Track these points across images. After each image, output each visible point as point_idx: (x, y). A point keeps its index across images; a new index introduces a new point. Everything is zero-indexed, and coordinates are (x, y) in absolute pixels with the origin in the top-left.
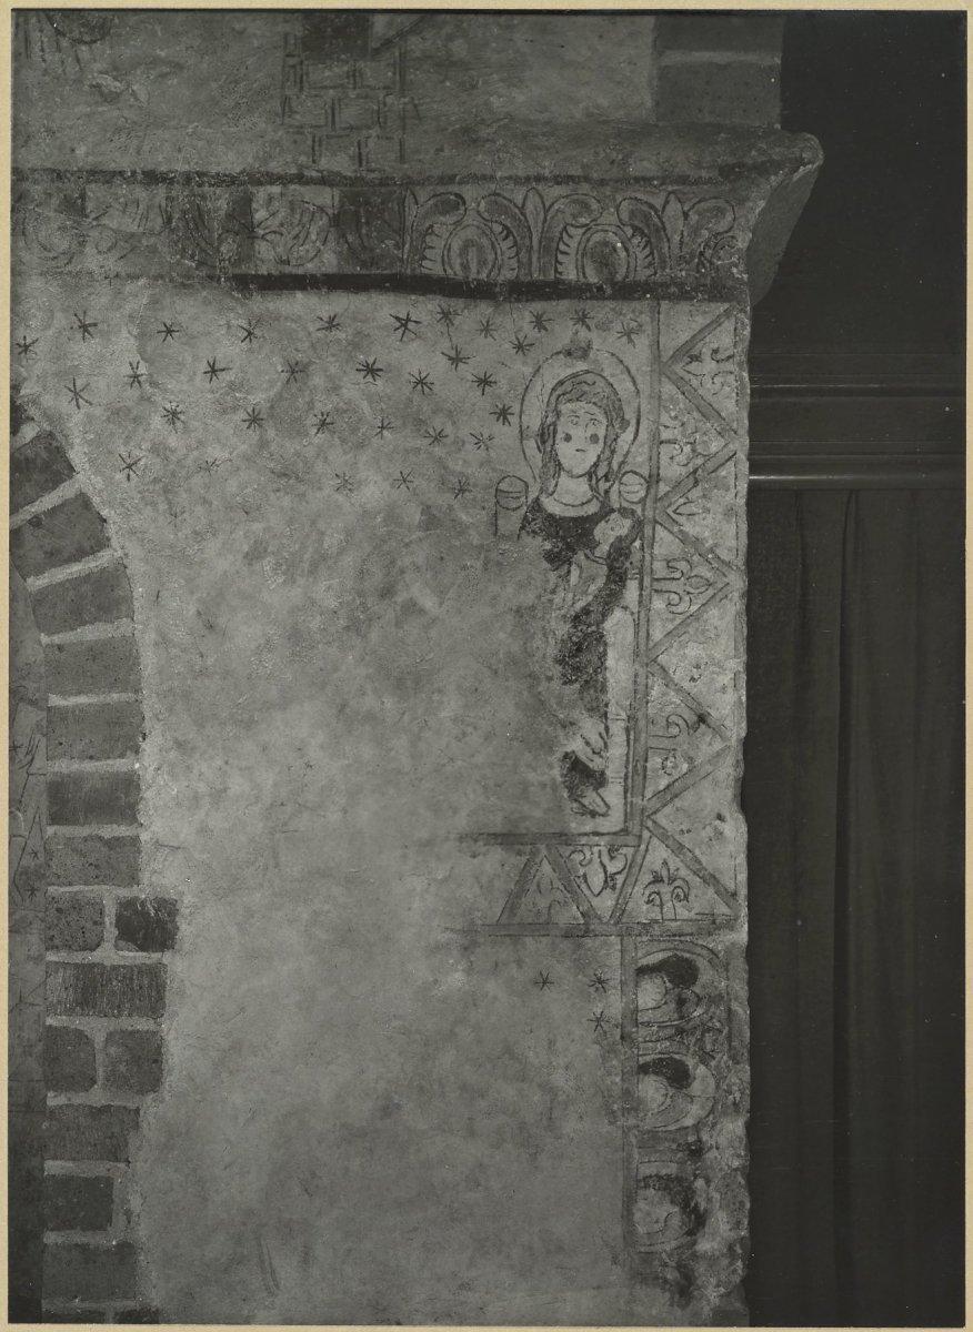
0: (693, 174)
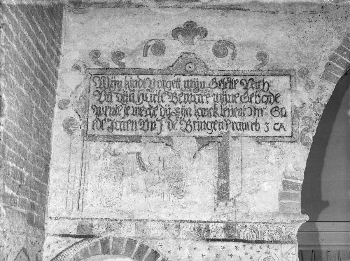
0: (287, 222)
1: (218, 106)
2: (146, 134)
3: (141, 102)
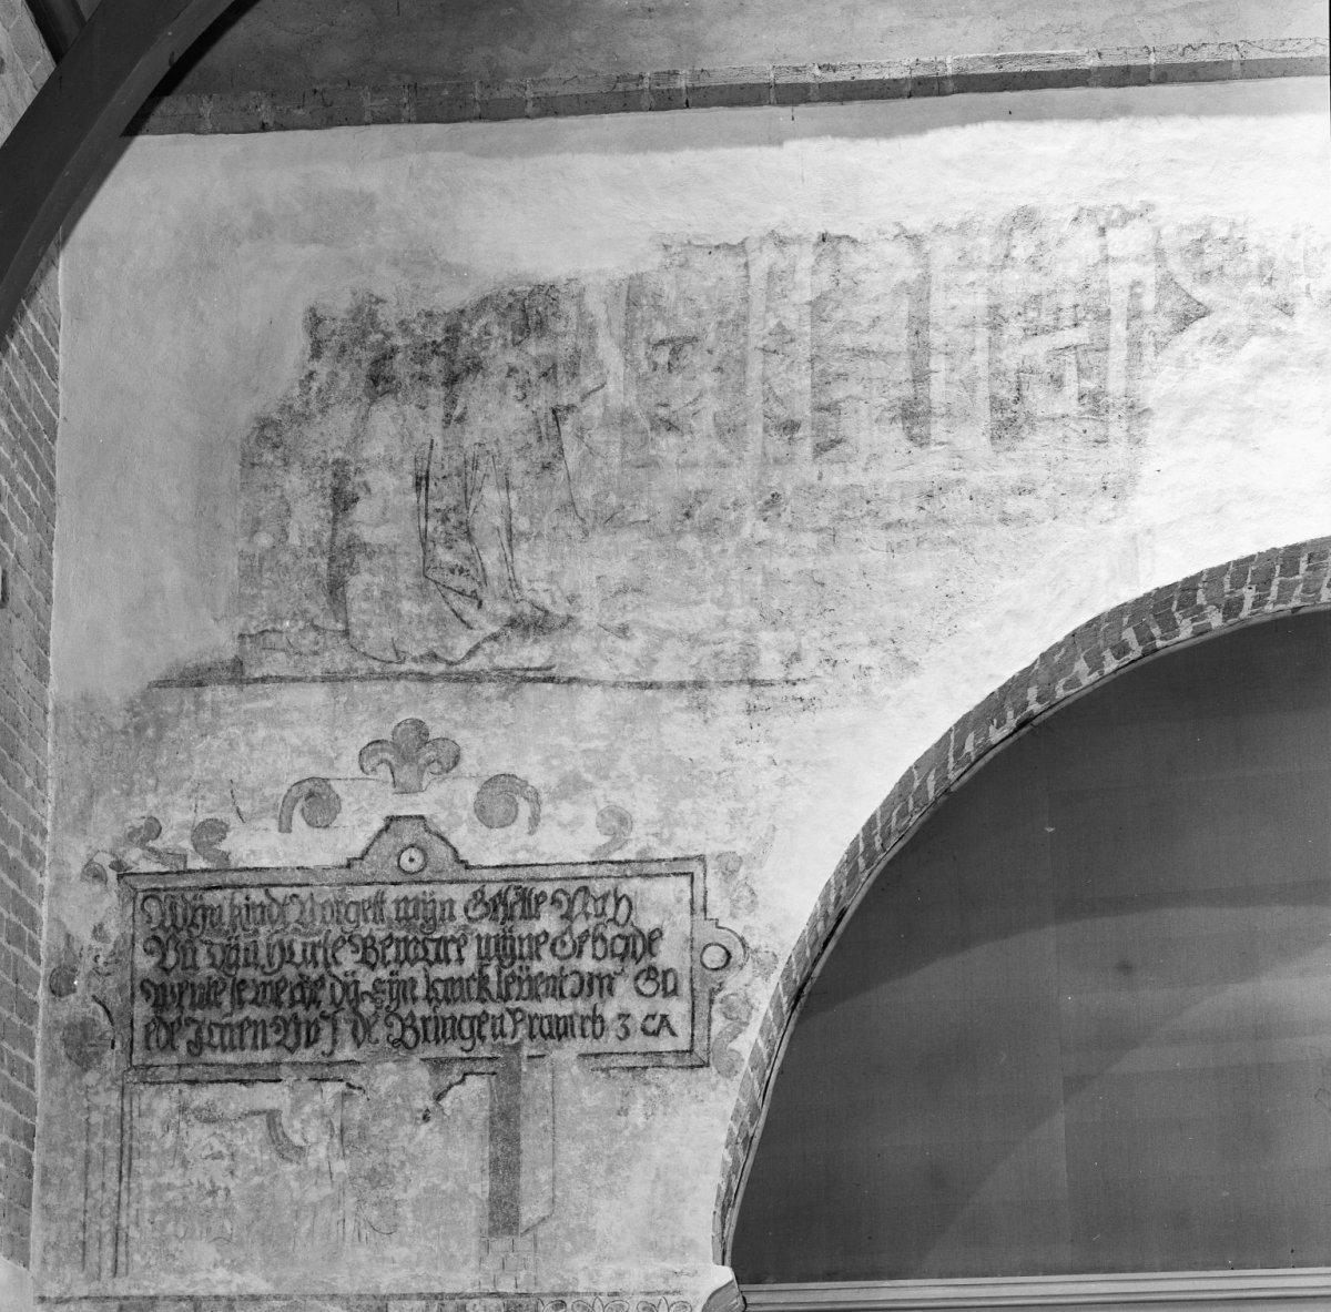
1: (491, 972)
2: (289, 1058)
3: (276, 967)
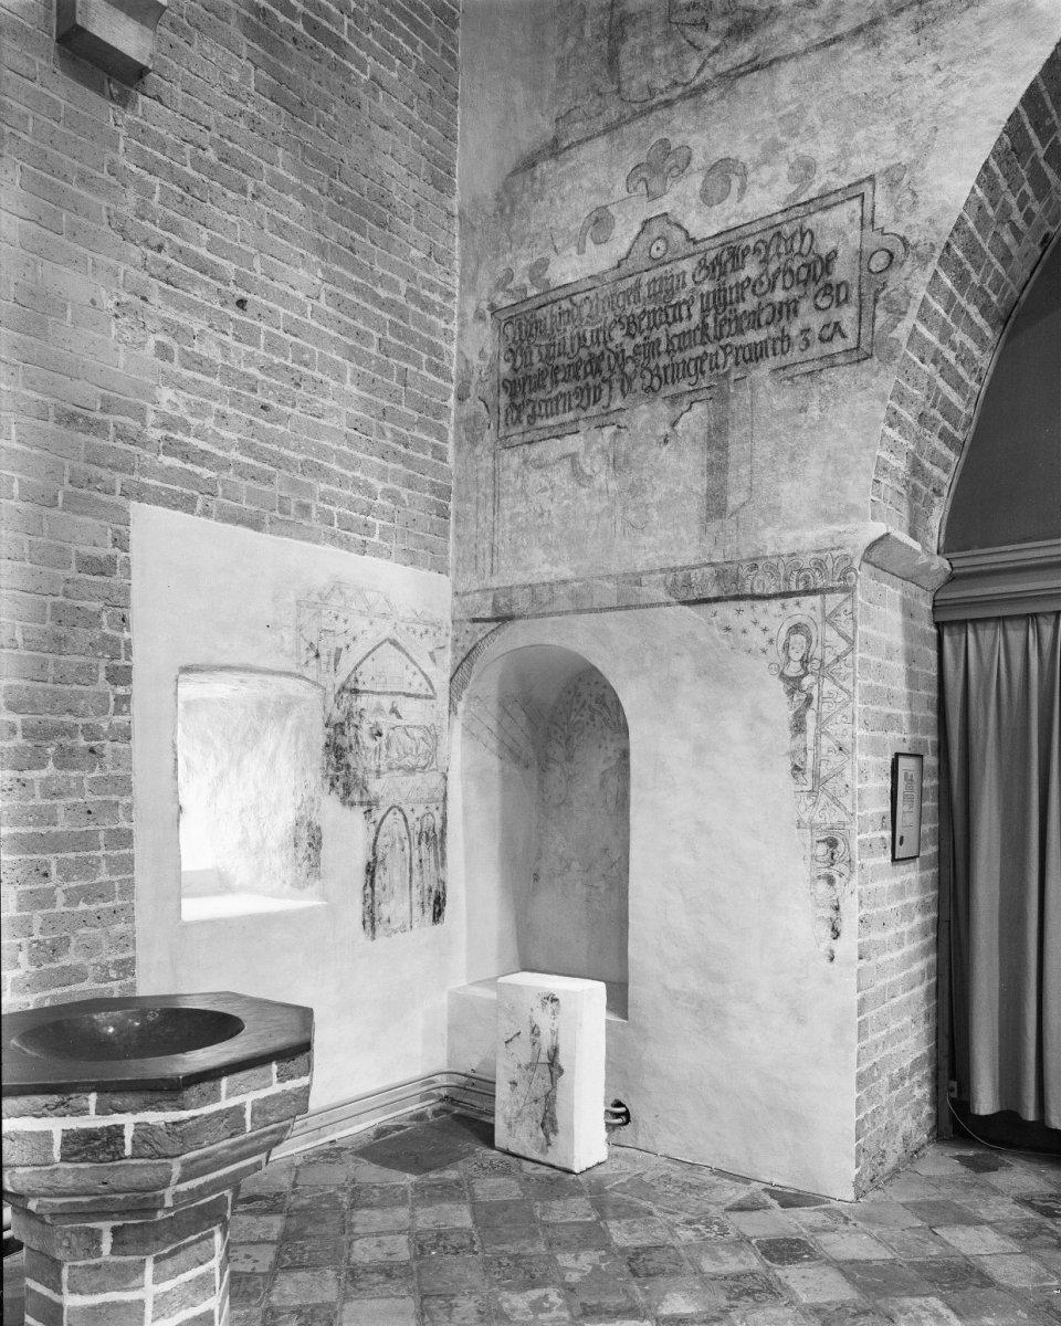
1: (710, 320)
2: (583, 415)
